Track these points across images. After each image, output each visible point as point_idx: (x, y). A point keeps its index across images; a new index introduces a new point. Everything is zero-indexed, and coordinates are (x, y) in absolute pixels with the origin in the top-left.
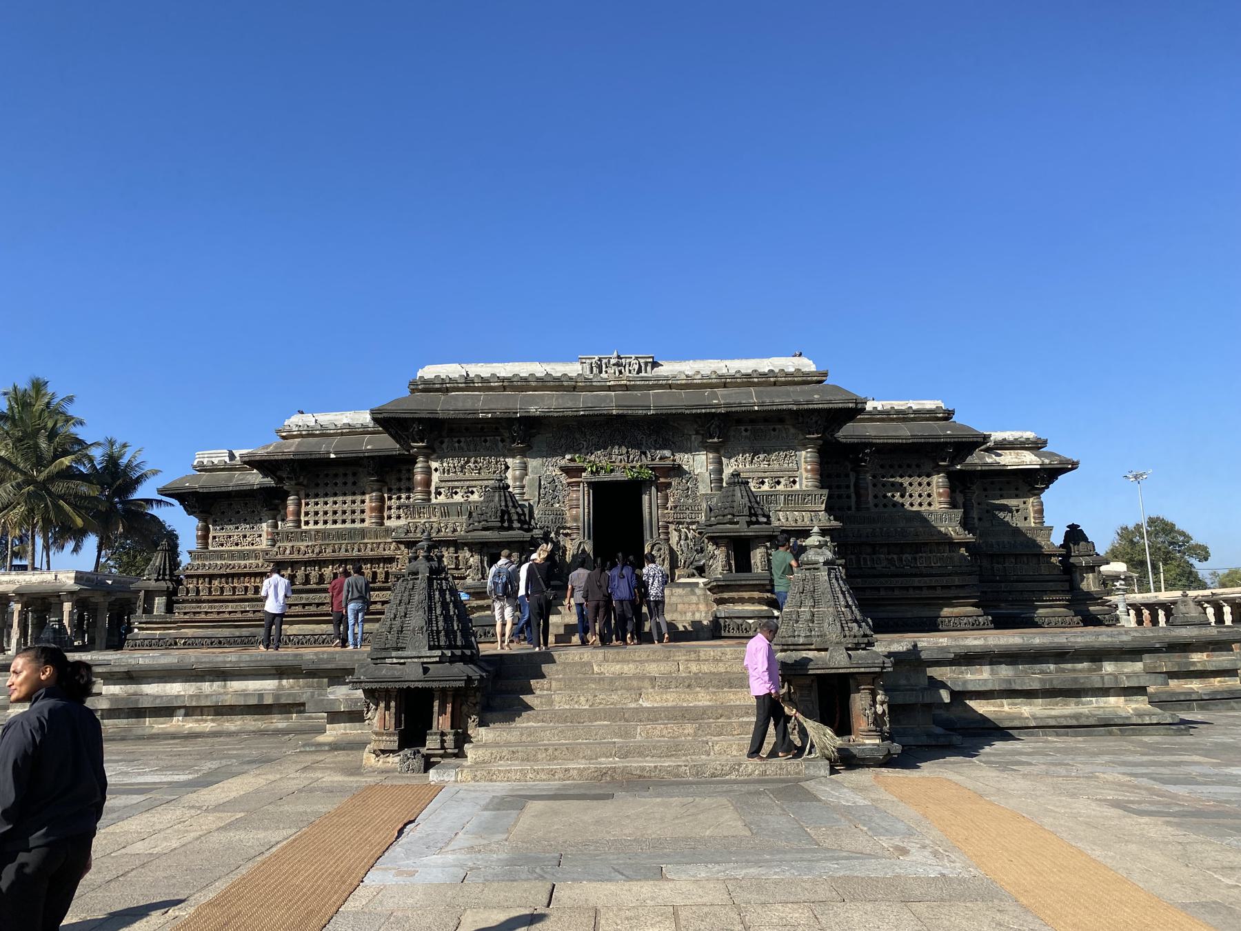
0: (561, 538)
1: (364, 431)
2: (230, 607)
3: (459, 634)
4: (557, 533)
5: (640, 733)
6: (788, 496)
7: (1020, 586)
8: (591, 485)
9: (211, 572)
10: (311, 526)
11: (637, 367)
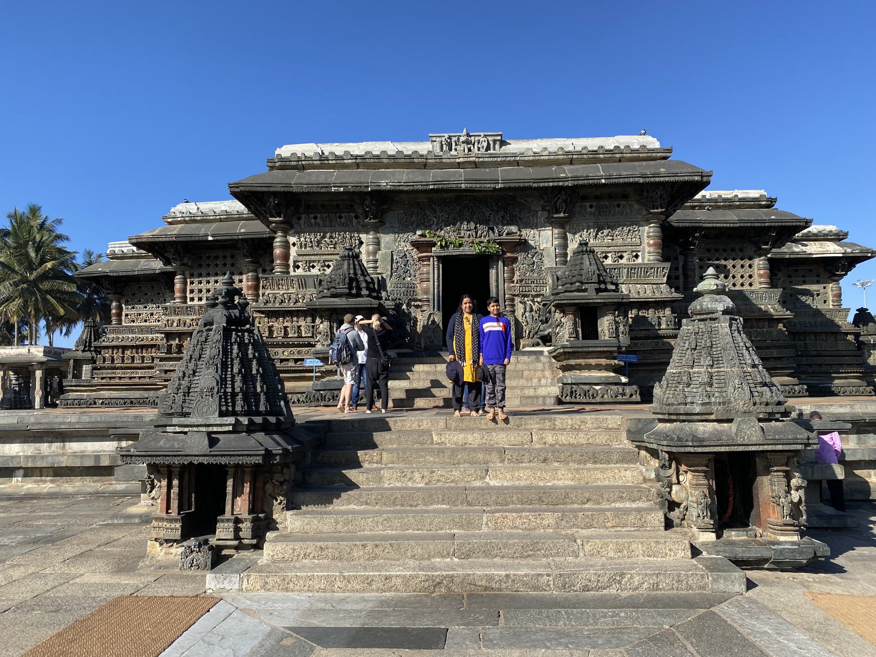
0: (412, 310)
1: (240, 218)
2: (140, 373)
4: (409, 305)
5: (486, 525)
6: (631, 269)
8: (441, 259)
9: (123, 343)
10: (196, 302)
11: (485, 145)
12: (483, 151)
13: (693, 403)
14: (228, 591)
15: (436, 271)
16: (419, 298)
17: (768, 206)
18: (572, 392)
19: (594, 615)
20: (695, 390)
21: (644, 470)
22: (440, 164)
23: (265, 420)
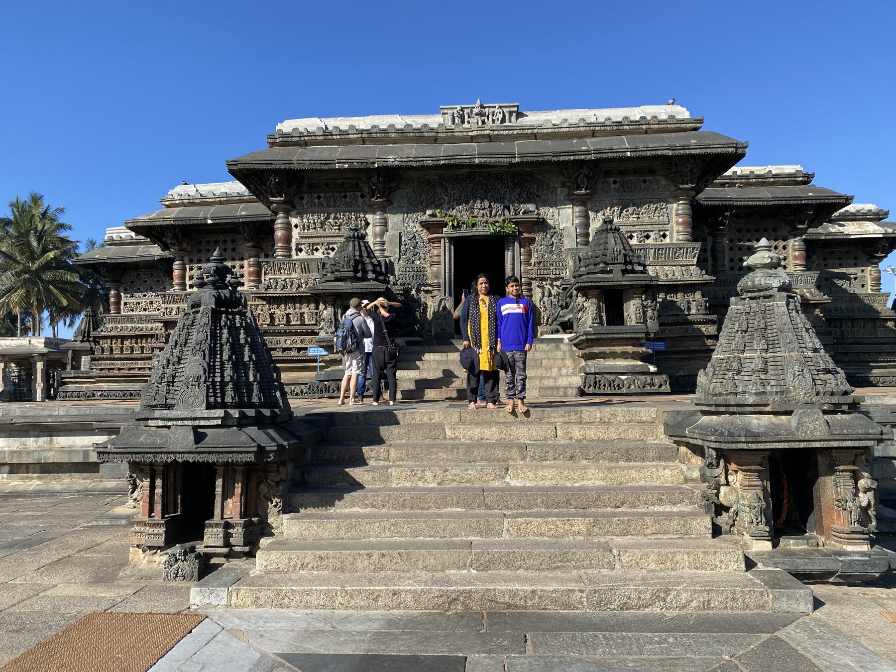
0: (422, 295)
1: (240, 200)
2: (140, 364)
3: (256, 387)
4: (418, 290)
5: (508, 531)
6: (658, 249)
7: (857, 348)
8: (453, 240)
9: (122, 333)
11: (500, 116)
12: (498, 123)
13: (744, 393)
14: (215, 606)
15: (447, 253)
16: (429, 282)
17: (805, 183)
18: (595, 383)
19: (638, 640)
20: (746, 378)
21: (685, 468)
22: (452, 139)
23: (259, 413)
